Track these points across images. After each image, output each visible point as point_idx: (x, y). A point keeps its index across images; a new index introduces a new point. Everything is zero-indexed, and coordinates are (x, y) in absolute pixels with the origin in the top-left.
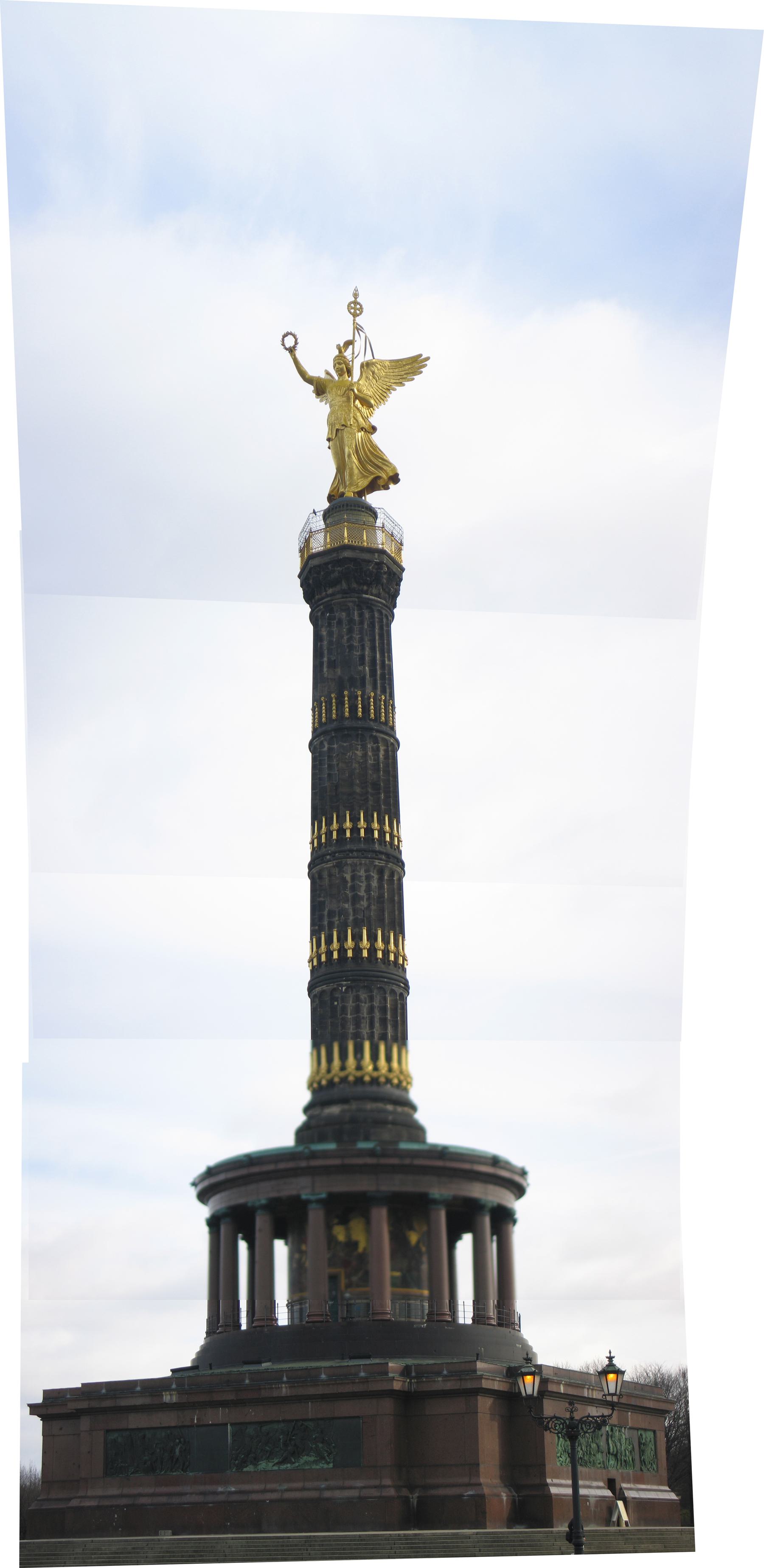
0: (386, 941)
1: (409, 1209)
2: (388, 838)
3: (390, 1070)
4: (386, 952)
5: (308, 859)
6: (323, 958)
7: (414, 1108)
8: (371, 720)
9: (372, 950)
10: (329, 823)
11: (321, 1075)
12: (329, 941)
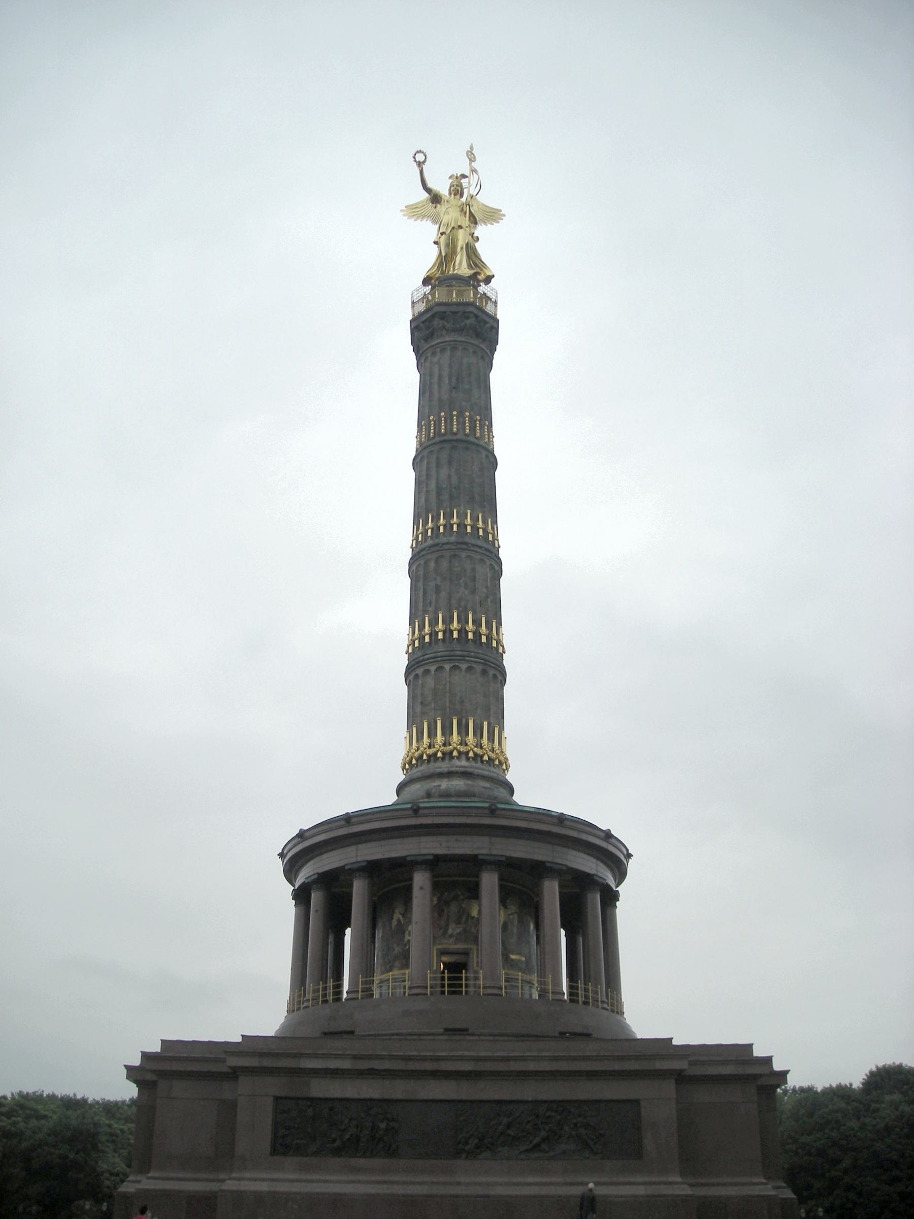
0: (489, 626)
1: (521, 885)
2: (491, 538)
3: (493, 750)
4: (490, 638)
5: (408, 554)
6: (427, 639)
7: (511, 790)
8: (477, 438)
9: (477, 634)
10: (436, 518)
11: (422, 749)
12: (434, 622)
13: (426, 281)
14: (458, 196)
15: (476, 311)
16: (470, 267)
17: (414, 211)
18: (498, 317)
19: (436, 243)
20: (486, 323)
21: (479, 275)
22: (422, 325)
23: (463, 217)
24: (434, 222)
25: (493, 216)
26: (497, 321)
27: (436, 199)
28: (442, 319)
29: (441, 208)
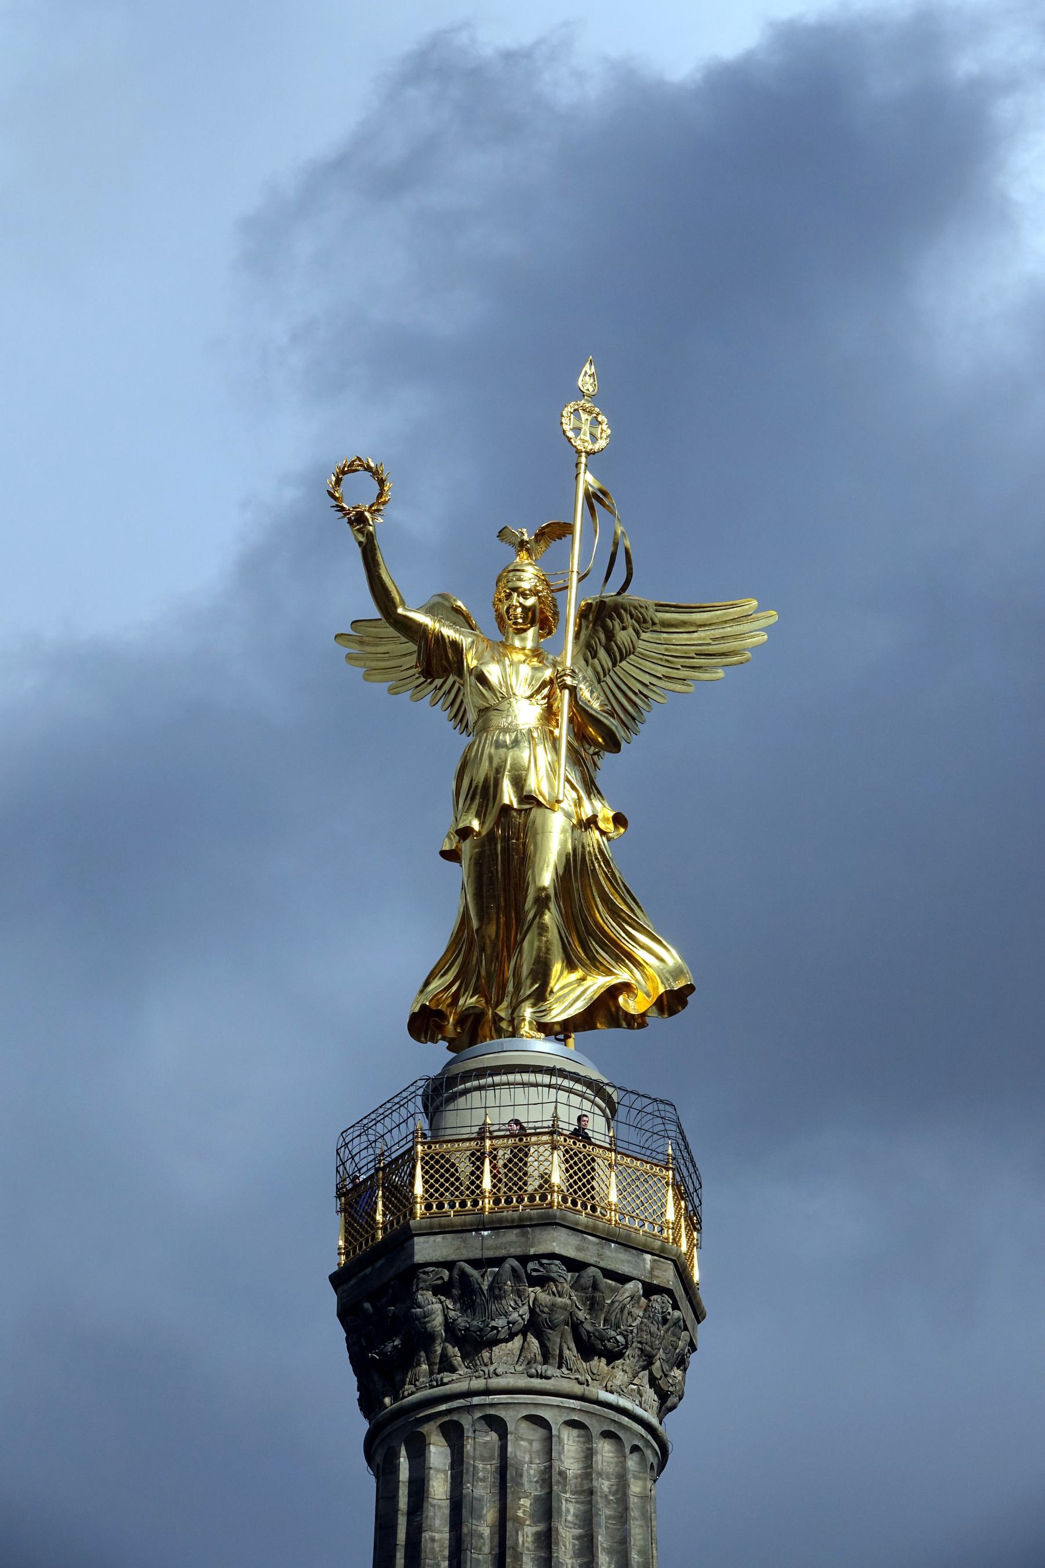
20: (624, 1279)
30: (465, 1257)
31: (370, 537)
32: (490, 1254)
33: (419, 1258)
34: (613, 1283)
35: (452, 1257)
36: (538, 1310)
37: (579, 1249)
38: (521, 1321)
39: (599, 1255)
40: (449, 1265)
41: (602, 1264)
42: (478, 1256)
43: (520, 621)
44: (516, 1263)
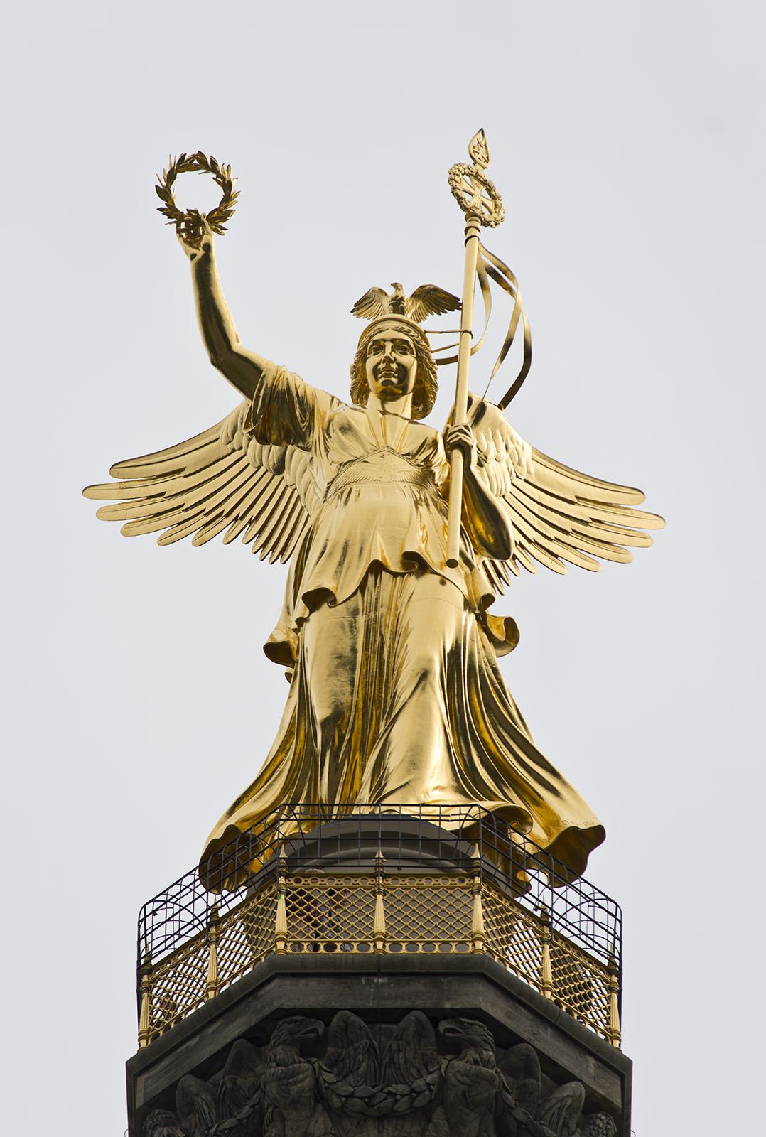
13: (224, 860)
14: (405, 405)
15: (498, 1009)
16: (466, 780)
17: (165, 495)
18: (628, 1047)
19: (278, 652)
20: (563, 1077)
21: (519, 838)
22: (192, 1083)
23: (428, 516)
24: (272, 547)
25: (589, 521)
26: (621, 1069)
27: (279, 416)
28: (309, 1049)
29: (309, 471)
30: (352, 1003)
31: (207, 248)
32: (389, 1004)
33: (287, 1004)
34: (548, 1078)
35: (334, 1004)
36: (453, 1079)
37: (508, 1015)
38: (427, 1093)
39: (533, 1034)
40: (325, 1014)
41: (537, 1044)
42: (371, 1004)
43: (395, 380)
44: (423, 1017)
